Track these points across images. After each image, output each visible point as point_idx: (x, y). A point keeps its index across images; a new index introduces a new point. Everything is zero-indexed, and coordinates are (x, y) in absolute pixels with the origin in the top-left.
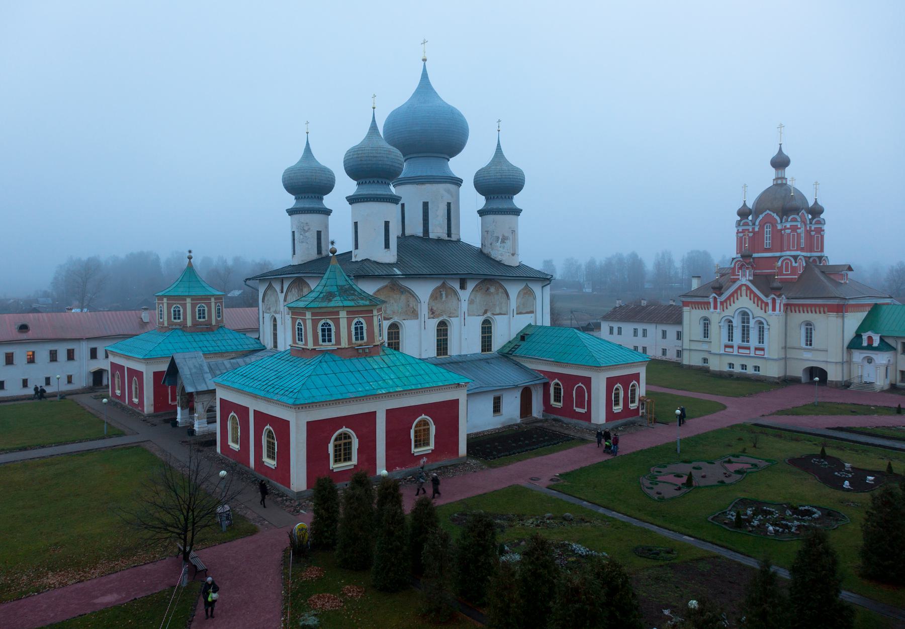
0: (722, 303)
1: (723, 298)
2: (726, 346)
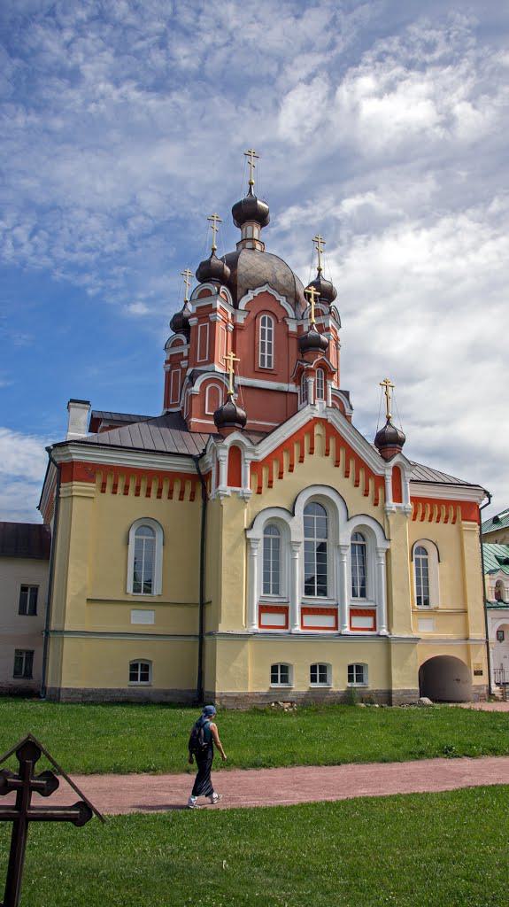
0: (255, 466)
1: (265, 448)
2: (263, 609)
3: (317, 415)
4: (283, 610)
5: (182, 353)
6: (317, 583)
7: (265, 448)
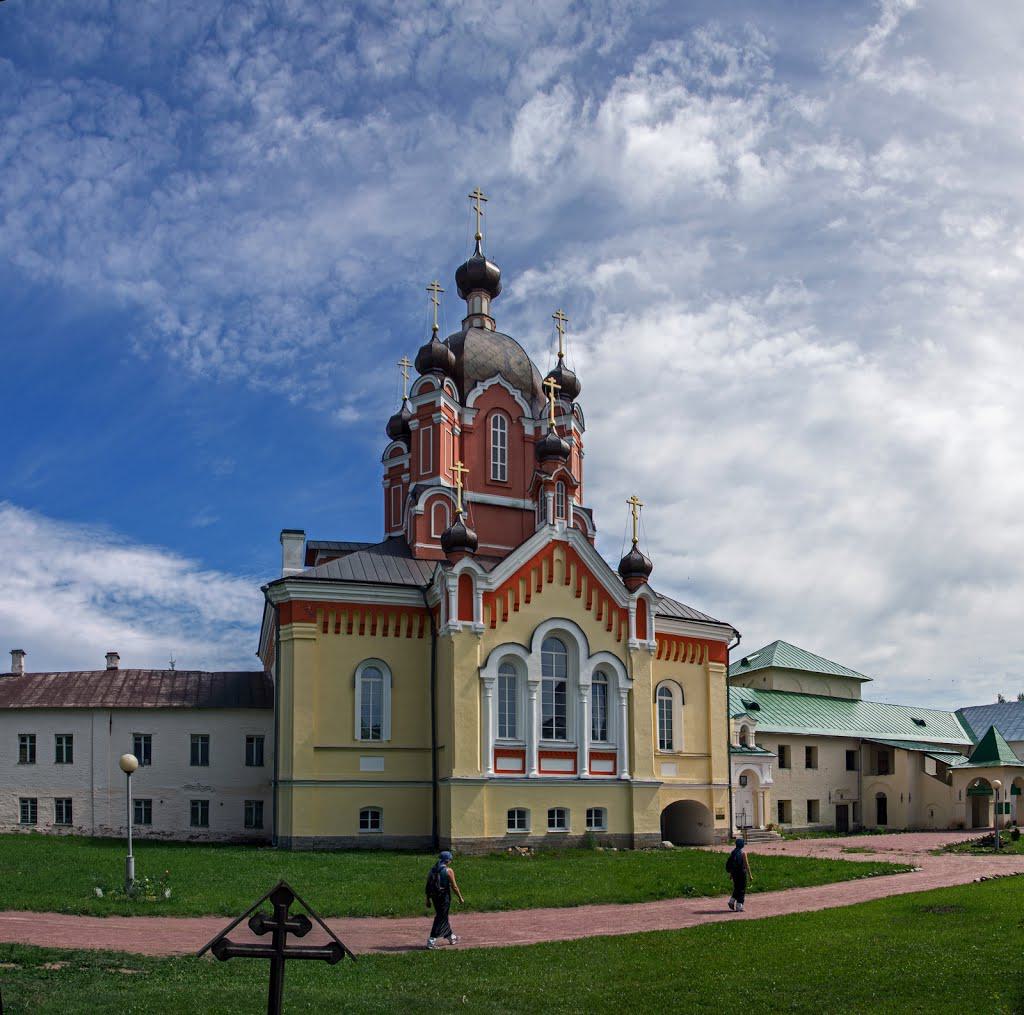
0: (489, 597)
1: (499, 576)
2: (499, 753)
3: (557, 536)
4: (520, 754)
5: (402, 465)
6: (556, 725)
7: (499, 576)
